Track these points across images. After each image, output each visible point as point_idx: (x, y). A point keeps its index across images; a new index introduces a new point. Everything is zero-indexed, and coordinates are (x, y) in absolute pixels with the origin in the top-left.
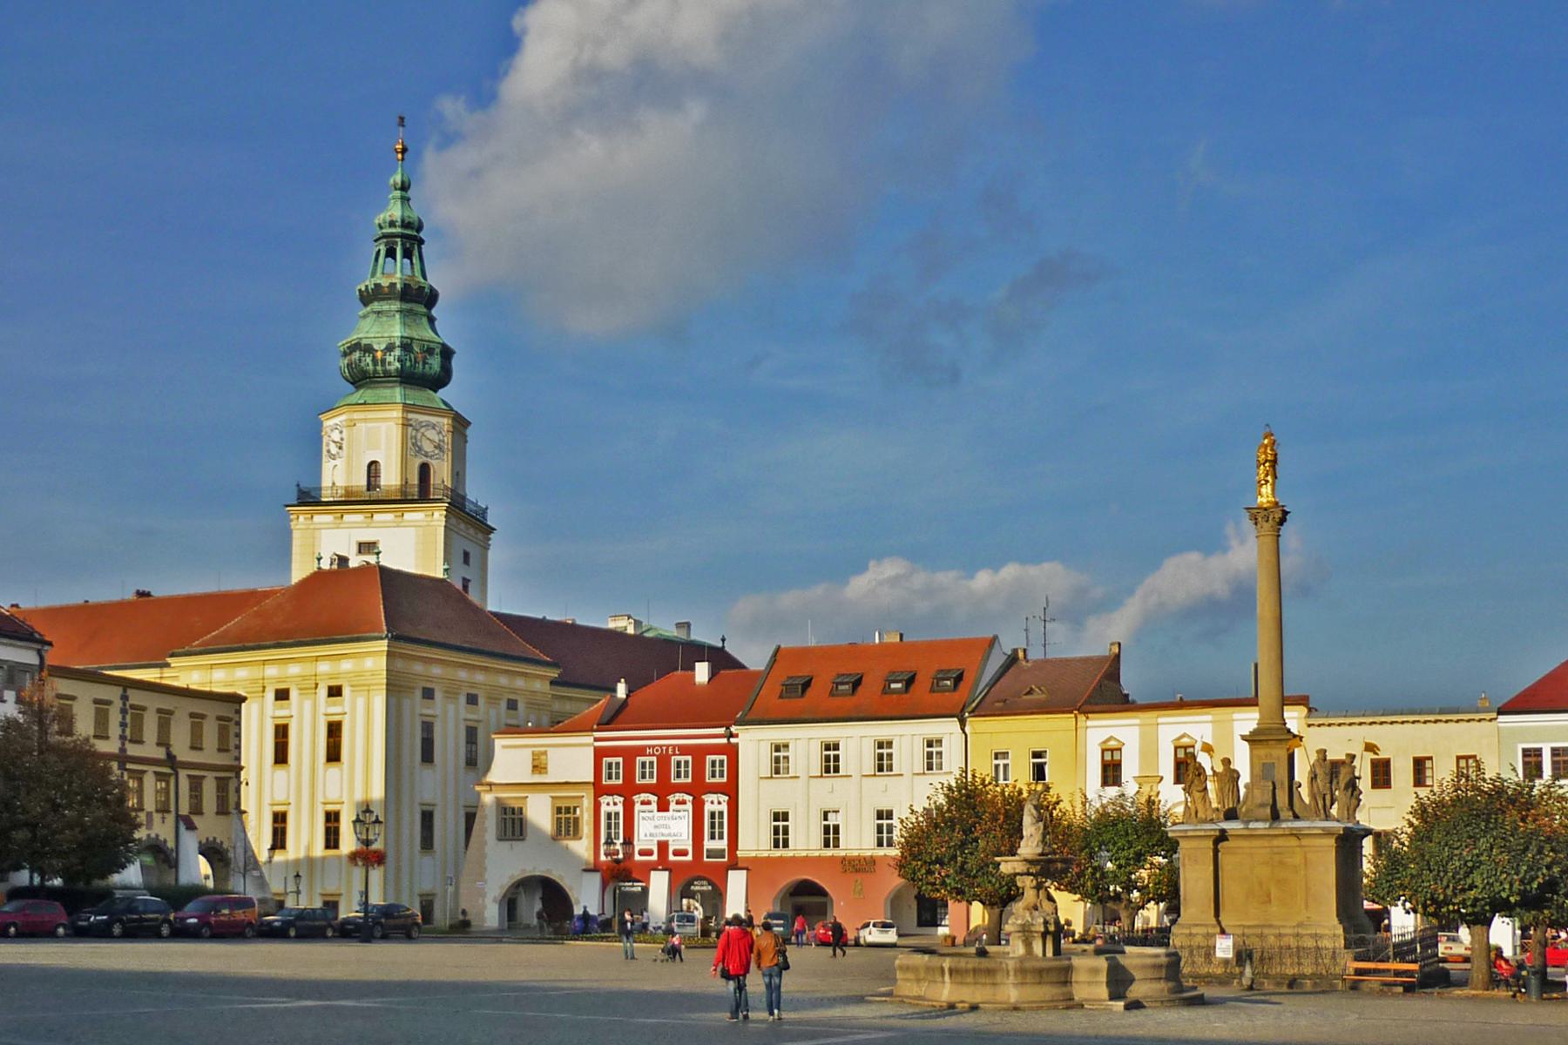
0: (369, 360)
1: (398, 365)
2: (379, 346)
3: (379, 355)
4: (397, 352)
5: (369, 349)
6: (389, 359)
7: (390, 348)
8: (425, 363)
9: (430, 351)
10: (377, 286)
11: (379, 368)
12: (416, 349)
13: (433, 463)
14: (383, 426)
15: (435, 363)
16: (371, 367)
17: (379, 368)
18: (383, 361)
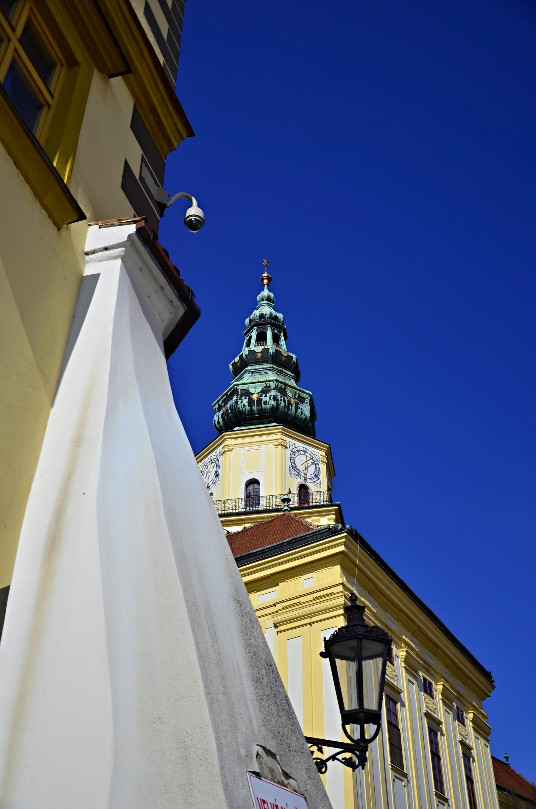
0: (245, 401)
1: (273, 403)
2: (256, 390)
3: (255, 397)
4: (273, 393)
5: (247, 393)
6: (264, 399)
7: (266, 391)
8: (297, 407)
9: (302, 400)
10: (252, 352)
11: (255, 408)
12: (290, 394)
13: (309, 484)
14: (263, 448)
15: (306, 410)
16: (247, 407)
17: (255, 408)
18: (259, 401)
